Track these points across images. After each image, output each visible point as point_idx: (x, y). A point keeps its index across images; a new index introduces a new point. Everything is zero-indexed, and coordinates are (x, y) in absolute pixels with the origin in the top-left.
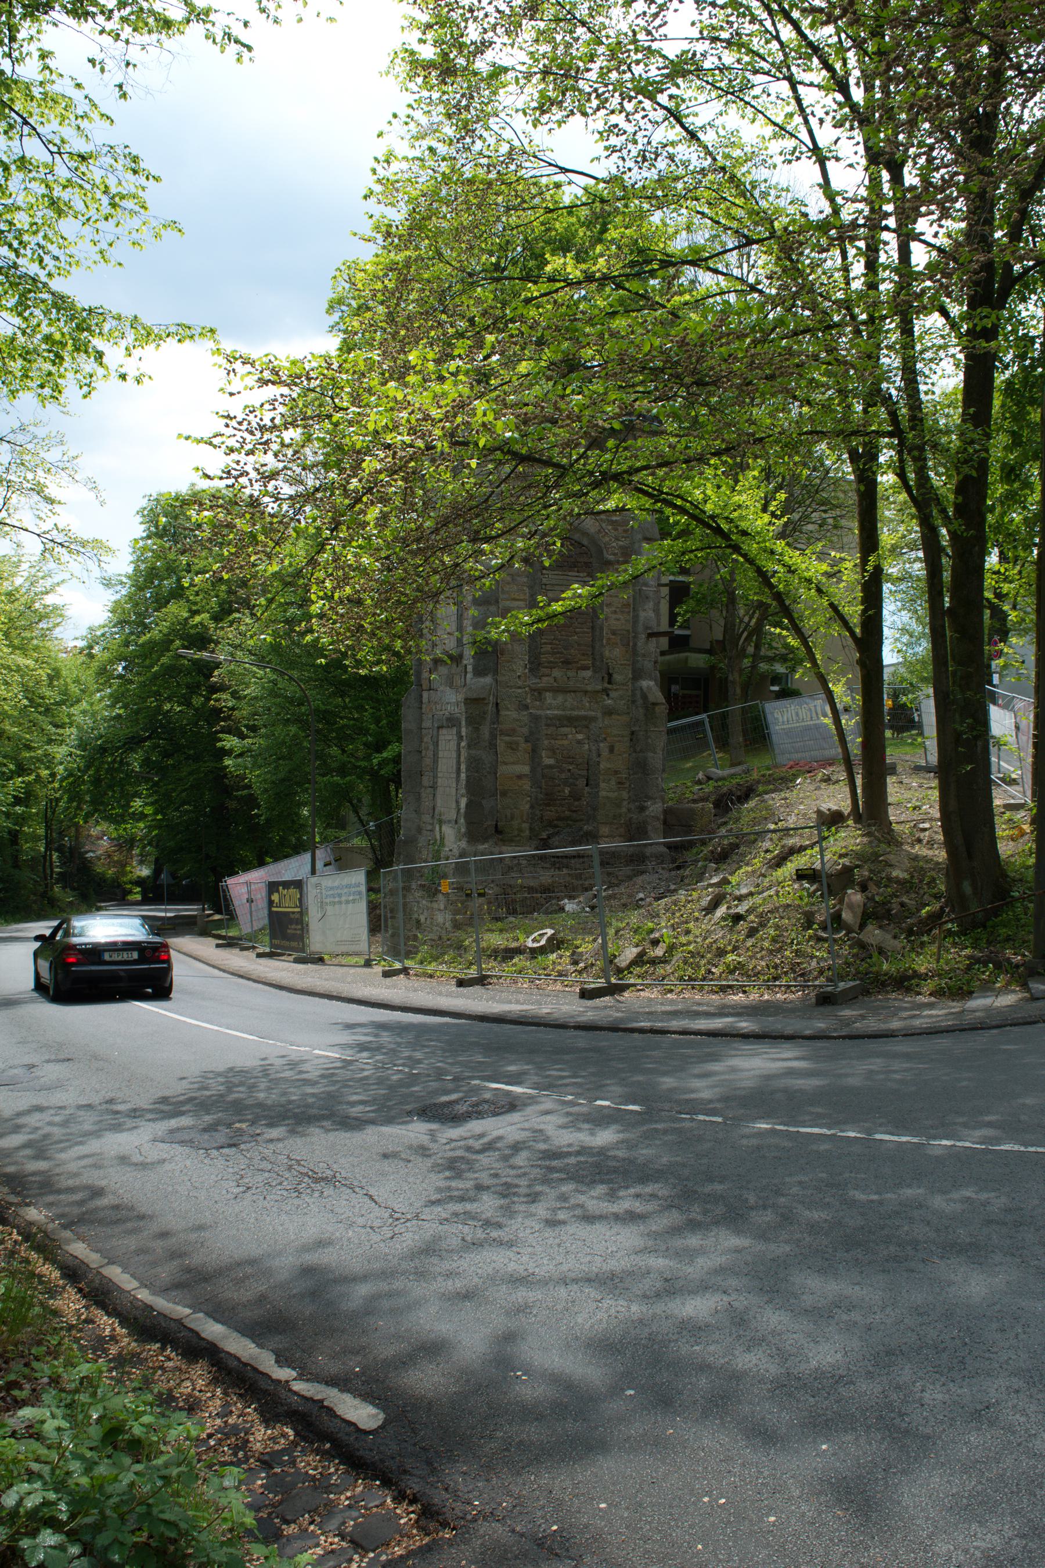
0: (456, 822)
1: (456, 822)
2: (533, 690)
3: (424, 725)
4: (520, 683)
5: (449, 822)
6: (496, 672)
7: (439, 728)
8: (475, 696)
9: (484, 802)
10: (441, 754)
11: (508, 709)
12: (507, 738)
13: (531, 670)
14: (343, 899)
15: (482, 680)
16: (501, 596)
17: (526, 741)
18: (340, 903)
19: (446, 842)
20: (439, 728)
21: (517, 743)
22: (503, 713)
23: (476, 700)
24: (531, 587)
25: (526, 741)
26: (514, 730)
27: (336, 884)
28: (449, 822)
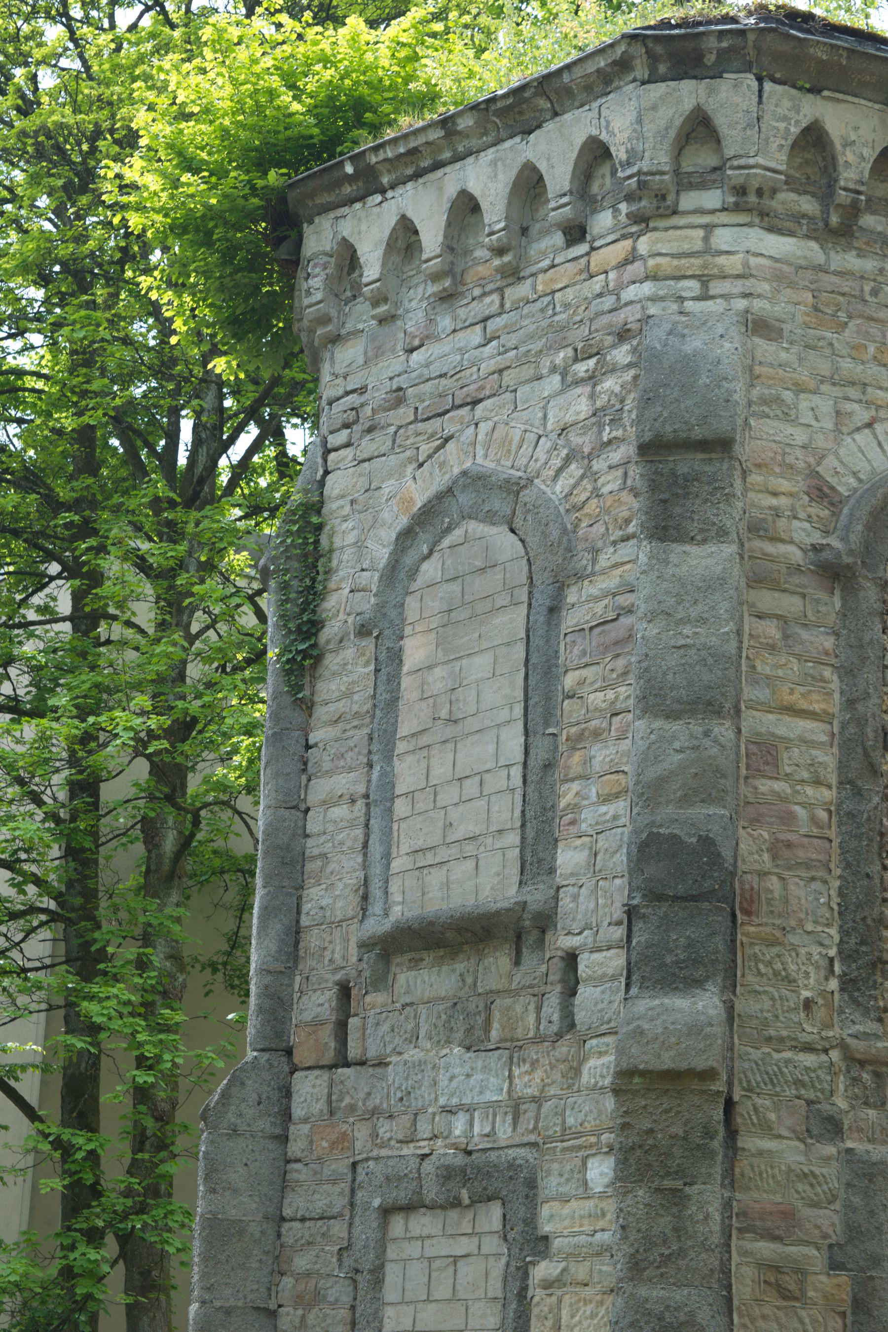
2: (854, 1061)
4: (810, 1031)
6: (731, 984)
7: (386, 1212)
8: (667, 1061)
11: (767, 1129)
12: (765, 1248)
13: (847, 984)
15: (680, 1003)
16: (749, 693)
17: (835, 1266)
20: (386, 1212)
21: (801, 1273)
22: (749, 1142)
23: (672, 1076)
24: (847, 672)
25: (835, 1266)
26: (789, 1215)
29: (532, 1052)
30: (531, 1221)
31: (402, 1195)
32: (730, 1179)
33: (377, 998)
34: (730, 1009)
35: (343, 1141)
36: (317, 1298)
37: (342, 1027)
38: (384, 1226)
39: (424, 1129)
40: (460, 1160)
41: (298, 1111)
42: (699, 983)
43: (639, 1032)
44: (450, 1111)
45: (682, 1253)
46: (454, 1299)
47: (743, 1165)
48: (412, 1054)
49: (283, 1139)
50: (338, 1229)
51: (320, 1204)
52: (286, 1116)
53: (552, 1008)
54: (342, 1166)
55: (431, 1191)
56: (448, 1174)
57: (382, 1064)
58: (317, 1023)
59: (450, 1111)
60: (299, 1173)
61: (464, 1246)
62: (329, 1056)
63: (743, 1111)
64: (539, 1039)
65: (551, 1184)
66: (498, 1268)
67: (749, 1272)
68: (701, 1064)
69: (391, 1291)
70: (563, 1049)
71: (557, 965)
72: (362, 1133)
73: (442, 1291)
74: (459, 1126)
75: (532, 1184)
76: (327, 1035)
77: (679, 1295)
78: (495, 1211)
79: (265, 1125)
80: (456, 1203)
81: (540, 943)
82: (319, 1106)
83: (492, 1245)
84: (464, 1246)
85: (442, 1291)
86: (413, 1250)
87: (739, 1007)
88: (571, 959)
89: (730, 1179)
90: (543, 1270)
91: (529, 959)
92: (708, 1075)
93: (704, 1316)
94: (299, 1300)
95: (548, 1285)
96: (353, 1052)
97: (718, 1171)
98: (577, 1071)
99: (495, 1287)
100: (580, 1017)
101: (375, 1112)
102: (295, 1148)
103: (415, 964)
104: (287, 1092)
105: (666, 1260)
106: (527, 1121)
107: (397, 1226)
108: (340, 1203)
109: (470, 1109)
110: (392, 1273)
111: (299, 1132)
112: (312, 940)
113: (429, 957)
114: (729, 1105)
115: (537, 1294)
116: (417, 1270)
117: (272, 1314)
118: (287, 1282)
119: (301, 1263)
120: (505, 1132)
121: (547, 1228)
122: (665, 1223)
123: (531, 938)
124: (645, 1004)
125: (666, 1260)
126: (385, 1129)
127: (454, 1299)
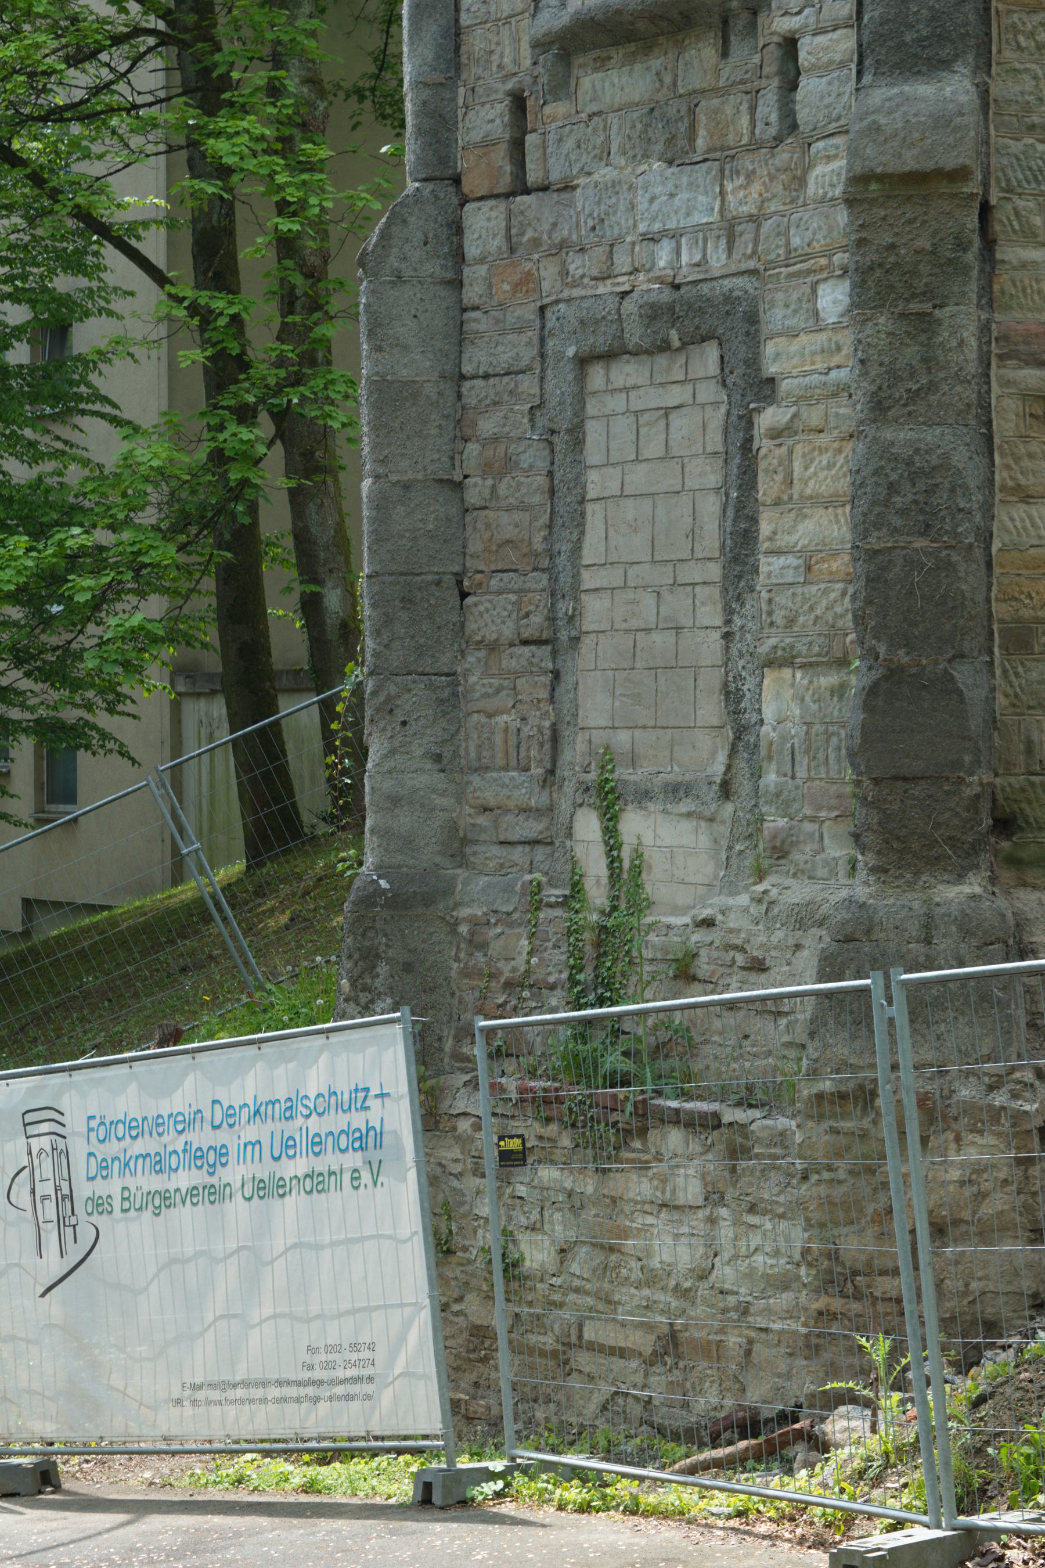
0: (726, 790)
1: (726, 790)
3: (476, 359)
5: (676, 791)
6: (985, 63)
7: (583, 362)
8: (910, 161)
9: (963, 675)
10: (595, 483)
14: (234, 1174)
18: (215, 1194)
19: (654, 885)
20: (583, 362)
22: (1009, 253)
23: (917, 179)
27: (179, 1102)
28: (676, 791)
29: (747, 163)
30: (753, 362)
31: (601, 341)
32: (988, 298)
33: (558, 109)
34: (984, 93)
35: (528, 282)
36: (509, 464)
37: (517, 147)
38: (581, 378)
39: (622, 261)
40: (667, 296)
41: (472, 250)
42: (945, 64)
43: (876, 128)
44: (651, 239)
45: (932, 387)
46: (667, 457)
47: (1003, 281)
48: (604, 174)
49: (457, 284)
50: (528, 385)
51: (505, 357)
52: (459, 256)
53: (769, 107)
54: (528, 312)
55: (635, 334)
56: (653, 313)
57: (568, 187)
58: (487, 144)
59: (651, 239)
60: (478, 323)
61: (676, 395)
62: (505, 182)
63: (1002, 215)
64: (755, 146)
65: (775, 317)
66: (716, 419)
67: (1012, 405)
68: (950, 161)
69: (593, 453)
70: (784, 155)
71: (773, 54)
72: (549, 271)
73: (653, 448)
74: (663, 255)
75: (752, 319)
76: (501, 158)
77: (930, 436)
78: (711, 353)
79: (434, 268)
80: (664, 347)
81: (752, 27)
82: (497, 243)
83: (709, 392)
84: (676, 395)
85: (653, 448)
86: (617, 403)
87: (995, 91)
88: (790, 45)
89: (988, 298)
90: (769, 417)
91: (739, 48)
92: (960, 174)
93: (960, 457)
94: (486, 468)
95: (776, 434)
96: (533, 176)
97: (973, 288)
98: (801, 182)
99: (715, 441)
100: (803, 115)
101: (563, 246)
102: (472, 294)
103: (602, 64)
104: (457, 229)
105: (915, 396)
106: (744, 245)
107: (597, 375)
108: (528, 355)
109: (675, 235)
110: (594, 431)
111: (475, 275)
112: (476, 43)
113: (617, 55)
114: (985, 210)
115: (763, 444)
116: (623, 426)
117: (458, 486)
118: (473, 449)
119: (487, 426)
120: (718, 259)
121: (772, 369)
122: (911, 353)
123: (739, 23)
124: (880, 94)
125: (915, 396)
126: (576, 265)
127: (667, 457)
